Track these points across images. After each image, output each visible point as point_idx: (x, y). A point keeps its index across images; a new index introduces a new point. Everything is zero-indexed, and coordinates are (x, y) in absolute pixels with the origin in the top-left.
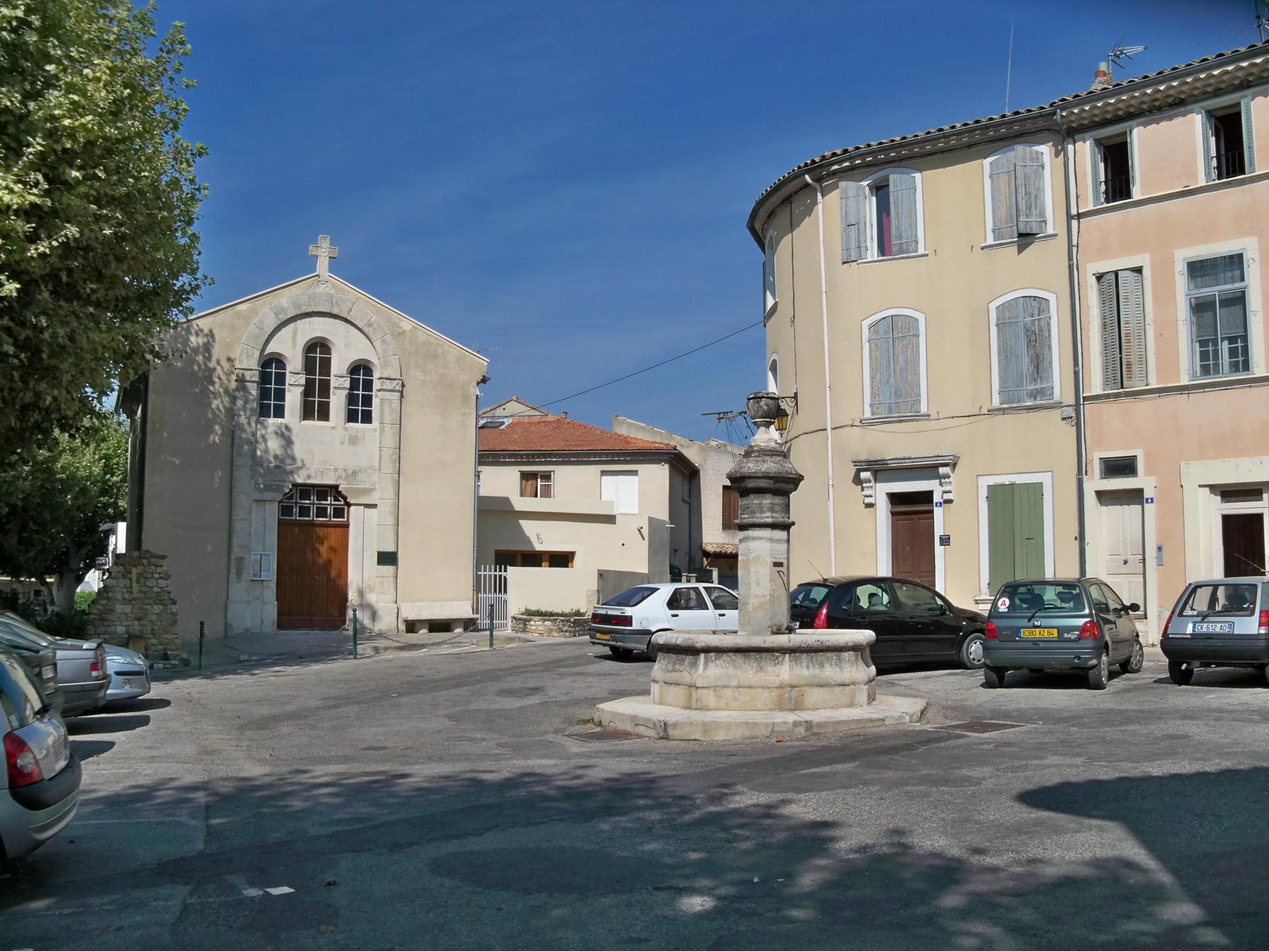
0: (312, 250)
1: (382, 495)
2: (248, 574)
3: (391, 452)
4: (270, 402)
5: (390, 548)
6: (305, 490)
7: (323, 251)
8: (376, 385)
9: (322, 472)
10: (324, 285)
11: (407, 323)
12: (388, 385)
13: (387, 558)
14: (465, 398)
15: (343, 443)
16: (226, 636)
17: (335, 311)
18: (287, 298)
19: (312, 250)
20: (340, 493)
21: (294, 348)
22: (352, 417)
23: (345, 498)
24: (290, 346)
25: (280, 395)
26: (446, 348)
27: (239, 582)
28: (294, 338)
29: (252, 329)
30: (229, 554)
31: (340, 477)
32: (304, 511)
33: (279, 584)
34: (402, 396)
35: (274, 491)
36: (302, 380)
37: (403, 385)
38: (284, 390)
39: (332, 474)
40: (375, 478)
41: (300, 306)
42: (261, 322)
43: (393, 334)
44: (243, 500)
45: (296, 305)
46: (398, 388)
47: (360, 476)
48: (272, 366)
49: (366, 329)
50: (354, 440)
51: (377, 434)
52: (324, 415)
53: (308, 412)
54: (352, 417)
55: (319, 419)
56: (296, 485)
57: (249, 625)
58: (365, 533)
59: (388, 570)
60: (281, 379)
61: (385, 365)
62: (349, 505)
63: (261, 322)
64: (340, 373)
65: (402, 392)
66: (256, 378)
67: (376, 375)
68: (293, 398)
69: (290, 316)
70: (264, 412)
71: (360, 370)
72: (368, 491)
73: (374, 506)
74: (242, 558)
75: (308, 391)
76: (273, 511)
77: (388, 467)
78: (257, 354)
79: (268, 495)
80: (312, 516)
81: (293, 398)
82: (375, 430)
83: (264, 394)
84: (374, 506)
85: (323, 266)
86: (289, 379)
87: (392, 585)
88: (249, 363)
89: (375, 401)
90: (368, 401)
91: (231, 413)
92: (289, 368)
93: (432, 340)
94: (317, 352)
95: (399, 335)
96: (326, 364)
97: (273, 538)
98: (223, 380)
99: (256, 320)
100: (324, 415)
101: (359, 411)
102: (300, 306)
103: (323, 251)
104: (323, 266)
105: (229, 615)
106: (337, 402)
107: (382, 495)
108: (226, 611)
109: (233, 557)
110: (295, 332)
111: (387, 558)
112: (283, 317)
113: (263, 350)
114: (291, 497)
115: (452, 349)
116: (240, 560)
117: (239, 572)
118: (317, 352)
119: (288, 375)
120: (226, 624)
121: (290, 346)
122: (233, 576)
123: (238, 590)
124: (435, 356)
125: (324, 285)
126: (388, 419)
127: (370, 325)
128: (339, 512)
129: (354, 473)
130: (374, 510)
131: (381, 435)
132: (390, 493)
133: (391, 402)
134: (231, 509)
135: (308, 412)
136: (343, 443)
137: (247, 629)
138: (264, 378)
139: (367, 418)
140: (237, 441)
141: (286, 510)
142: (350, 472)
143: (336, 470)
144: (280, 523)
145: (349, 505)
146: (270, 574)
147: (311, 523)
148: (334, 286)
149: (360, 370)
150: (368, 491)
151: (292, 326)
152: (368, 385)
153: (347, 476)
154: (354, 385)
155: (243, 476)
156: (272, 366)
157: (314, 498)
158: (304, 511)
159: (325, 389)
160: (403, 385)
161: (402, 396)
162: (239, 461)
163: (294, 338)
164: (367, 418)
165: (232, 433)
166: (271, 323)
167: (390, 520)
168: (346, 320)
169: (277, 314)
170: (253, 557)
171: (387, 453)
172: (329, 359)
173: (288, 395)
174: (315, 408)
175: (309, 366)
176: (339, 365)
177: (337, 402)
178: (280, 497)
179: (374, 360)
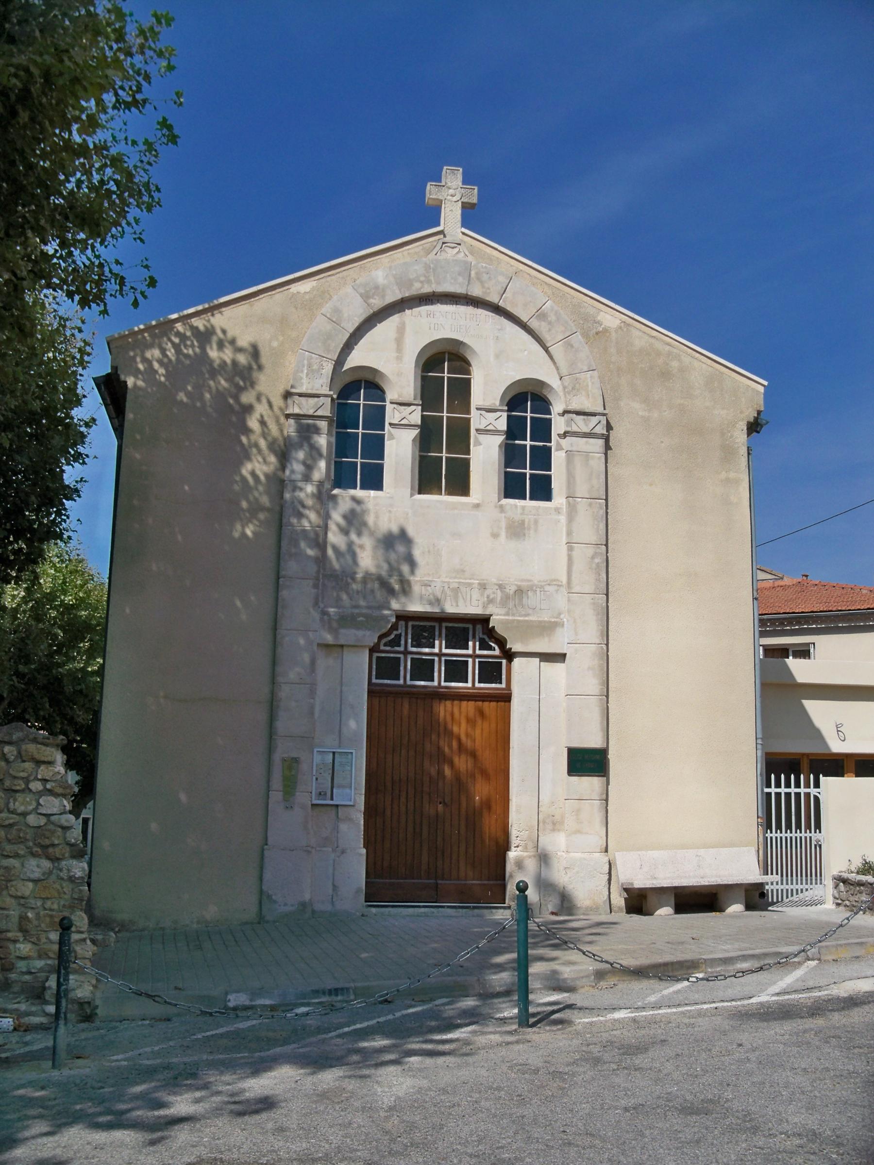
0: (432, 192)
1: (576, 635)
2: (305, 796)
3: (590, 551)
4: (357, 461)
5: (594, 742)
6: (426, 626)
7: (451, 192)
8: (558, 425)
9: (456, 591)
10: (454, 249)
11: (611, 316)
12: (581, 424)
13: (588, 762)
14: (728, 452)
15: (495, 536)
16: (261, 919)
17: (476, 291)
18: (385, 270)
19: (432, 192)
20: (491, 633)
21: (399, 359)
22: (513, 488)
23: (501, 643)
24: (393, 356)
25: (376, 447)
26: (686, 360)
27: (289, 808)
28: (399, 341)
29: (320, 324)
30: (270, 750)
31: (491, 601)
32: (423, 669)
33: (371, 812)
34: (608, 447)
35: (358, 626)
36: (415, 416)
37: (609, 427)
38: (382, 438)
39: (476, 594)
40: (561, 601)
41: (410, 283)
42: (337, 311)
43: (586, 335)
44: (298, 643)
45: (401, 282)
46: (601, 430)
47: (532, 600)
48: (358, 391)
49: (534, 324)
50: (517, 530)
51: (563, 519)
52: (460, 484)
53: (427, 478)
54: (513, 488)
55: (450, 492)
56: (404, 617)
57: (307, 897)
58: (545, 710)
59: (590, 784)
60: (377, 418)
61: (573, 389)
62: (509, 655)
63: (337, 311)
64: (487, 404)
65: (607, 439)
66: (326, 411)
67: (557, 407)
68: (400, 449)
69: (390, 299)
70: (342, 477)
71: (527, 403)
72: (548, 628)
73: (561, 657)
74: (296, 760)
75: (428, 435)
76: (359, 667)
77: (586, 581)
78: (328, 368)
79: (348, 635)
80: (439, 680)
81: (400, 449)
82: (558, 510)
83: (344, 445)
84: (561, 657)
85: (451, 217)
86: (392, 414)
87: (598, 817)
88: (318, 381)
89: (558, 458)
90: (543, 458)
91: (279, 483)
92: (391, 395)
93: (658, 346)
94: (444, 369)
95: (597, 336)
96: (462, 391)
97: (357, 725)
98: (265, 419)
99: (327, 308)
100: (460, 484)
101: (527, 476)
102: (410, 283)
103: (451, 192)
104: (451, 217)
105: (267, 876)
106: (485, 456)
107: (576, 635)
108: (262, 868)
109: (277, 757)
110: (401, 330)
111: (588, 762)
112: (378, 303)
113: (339, 362)
114: (396, 642)
115: (697, 363)
116: (292, 763)
117: (290, 786)
118: (444, 369)
119: (389, 408)
120: (261, 892)
121: (393, 356)
122: (276, 796)
123: (287, 824)
124: (665, 375)
125: (454, 249)
126: (582, 489)
127: (541, 315)
128: (491, 672)
129: (520, 592)
130: (559, 667)
131: (571, 519)
132: (591, 632)
133: (587, 455)
134: (274, 663)
135: (427, 478)
136: (495, 536)
137: (303, 905)
138: (343, 417)
139: (542, 490)
140: (286, 530)
141: (386, 667)
142: (510, 590)
143: (483, 586)
144: (373, 692)
145: (509, 655)
146: (354, 794)
147: (435, 690)
148: (472, 251)
149: (527, 403)
150: (548, 628)
151: (391, 323)
152: (543, 430)
153: (506, 598)
154: (514, 430)
155: (299, 598)
156: (358, 391)
157: (439, 646)
158: (423, 669)
159: (461, 436)
160: (609, 427)
161: (608, 447)
162: (291, 567)
163: (399, 341)
164: (542, 490)
165: (281, 512)
166: (355, 313)
167: (593, 685)
168: (497, 309)
169: (366, 297)
170: (317, 758)
171: (582, 554)
172: (468, 382)
173: (389, 447)
174: (441, 471)
175: (429, 393)
176: (487, 387)
177: (485, 456)
178: (371, 638)
179: (550, 378)
